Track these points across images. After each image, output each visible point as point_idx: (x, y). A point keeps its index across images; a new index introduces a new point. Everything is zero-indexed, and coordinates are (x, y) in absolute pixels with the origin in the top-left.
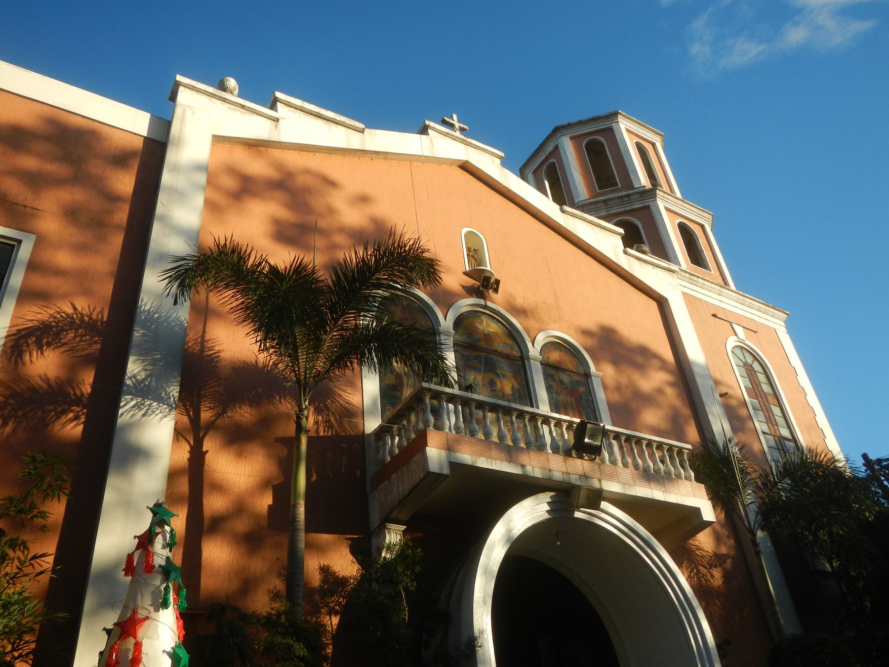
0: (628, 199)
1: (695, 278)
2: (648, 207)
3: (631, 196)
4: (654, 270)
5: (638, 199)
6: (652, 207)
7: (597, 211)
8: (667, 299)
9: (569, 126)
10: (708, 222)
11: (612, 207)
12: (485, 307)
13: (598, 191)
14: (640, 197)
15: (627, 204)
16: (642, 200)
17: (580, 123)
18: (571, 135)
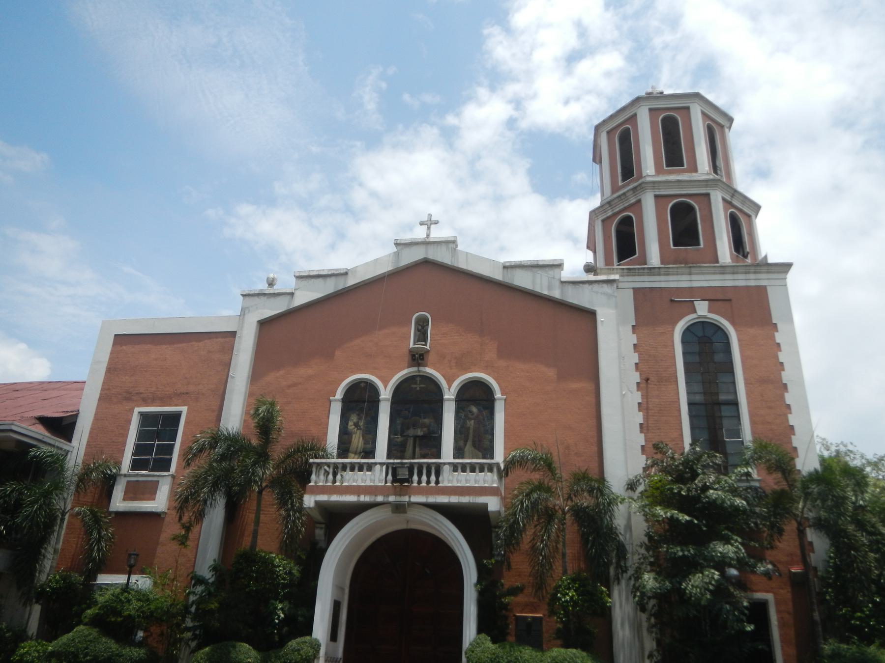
0: (624, 197)
1: (657, 270)
2: (639, 202)
3: (627, 194)
4: (591, 286)
5: (632, 195)
6: (642, 200)
7: (605, 212)
8: (595, 311)
9: (604, 122)
10: (717, 187)
11: (614, 207)
12: (419, 371)
13: (620, 184)
14: (634, 193)
15: (625, 201)
16: (635, 195)
17: (612, 117)
18: (607, 130)
